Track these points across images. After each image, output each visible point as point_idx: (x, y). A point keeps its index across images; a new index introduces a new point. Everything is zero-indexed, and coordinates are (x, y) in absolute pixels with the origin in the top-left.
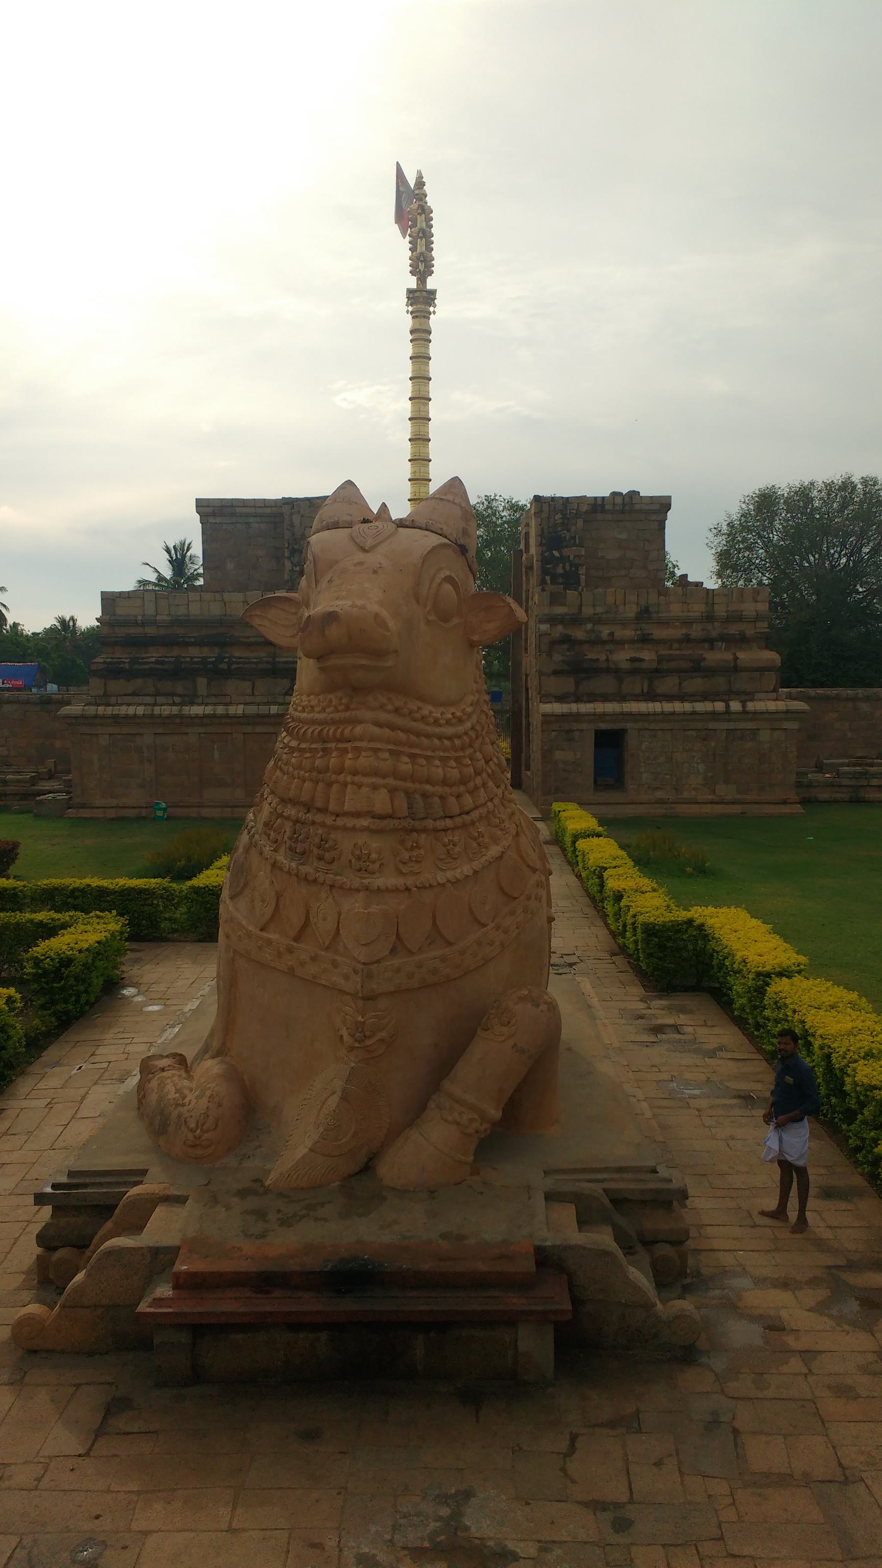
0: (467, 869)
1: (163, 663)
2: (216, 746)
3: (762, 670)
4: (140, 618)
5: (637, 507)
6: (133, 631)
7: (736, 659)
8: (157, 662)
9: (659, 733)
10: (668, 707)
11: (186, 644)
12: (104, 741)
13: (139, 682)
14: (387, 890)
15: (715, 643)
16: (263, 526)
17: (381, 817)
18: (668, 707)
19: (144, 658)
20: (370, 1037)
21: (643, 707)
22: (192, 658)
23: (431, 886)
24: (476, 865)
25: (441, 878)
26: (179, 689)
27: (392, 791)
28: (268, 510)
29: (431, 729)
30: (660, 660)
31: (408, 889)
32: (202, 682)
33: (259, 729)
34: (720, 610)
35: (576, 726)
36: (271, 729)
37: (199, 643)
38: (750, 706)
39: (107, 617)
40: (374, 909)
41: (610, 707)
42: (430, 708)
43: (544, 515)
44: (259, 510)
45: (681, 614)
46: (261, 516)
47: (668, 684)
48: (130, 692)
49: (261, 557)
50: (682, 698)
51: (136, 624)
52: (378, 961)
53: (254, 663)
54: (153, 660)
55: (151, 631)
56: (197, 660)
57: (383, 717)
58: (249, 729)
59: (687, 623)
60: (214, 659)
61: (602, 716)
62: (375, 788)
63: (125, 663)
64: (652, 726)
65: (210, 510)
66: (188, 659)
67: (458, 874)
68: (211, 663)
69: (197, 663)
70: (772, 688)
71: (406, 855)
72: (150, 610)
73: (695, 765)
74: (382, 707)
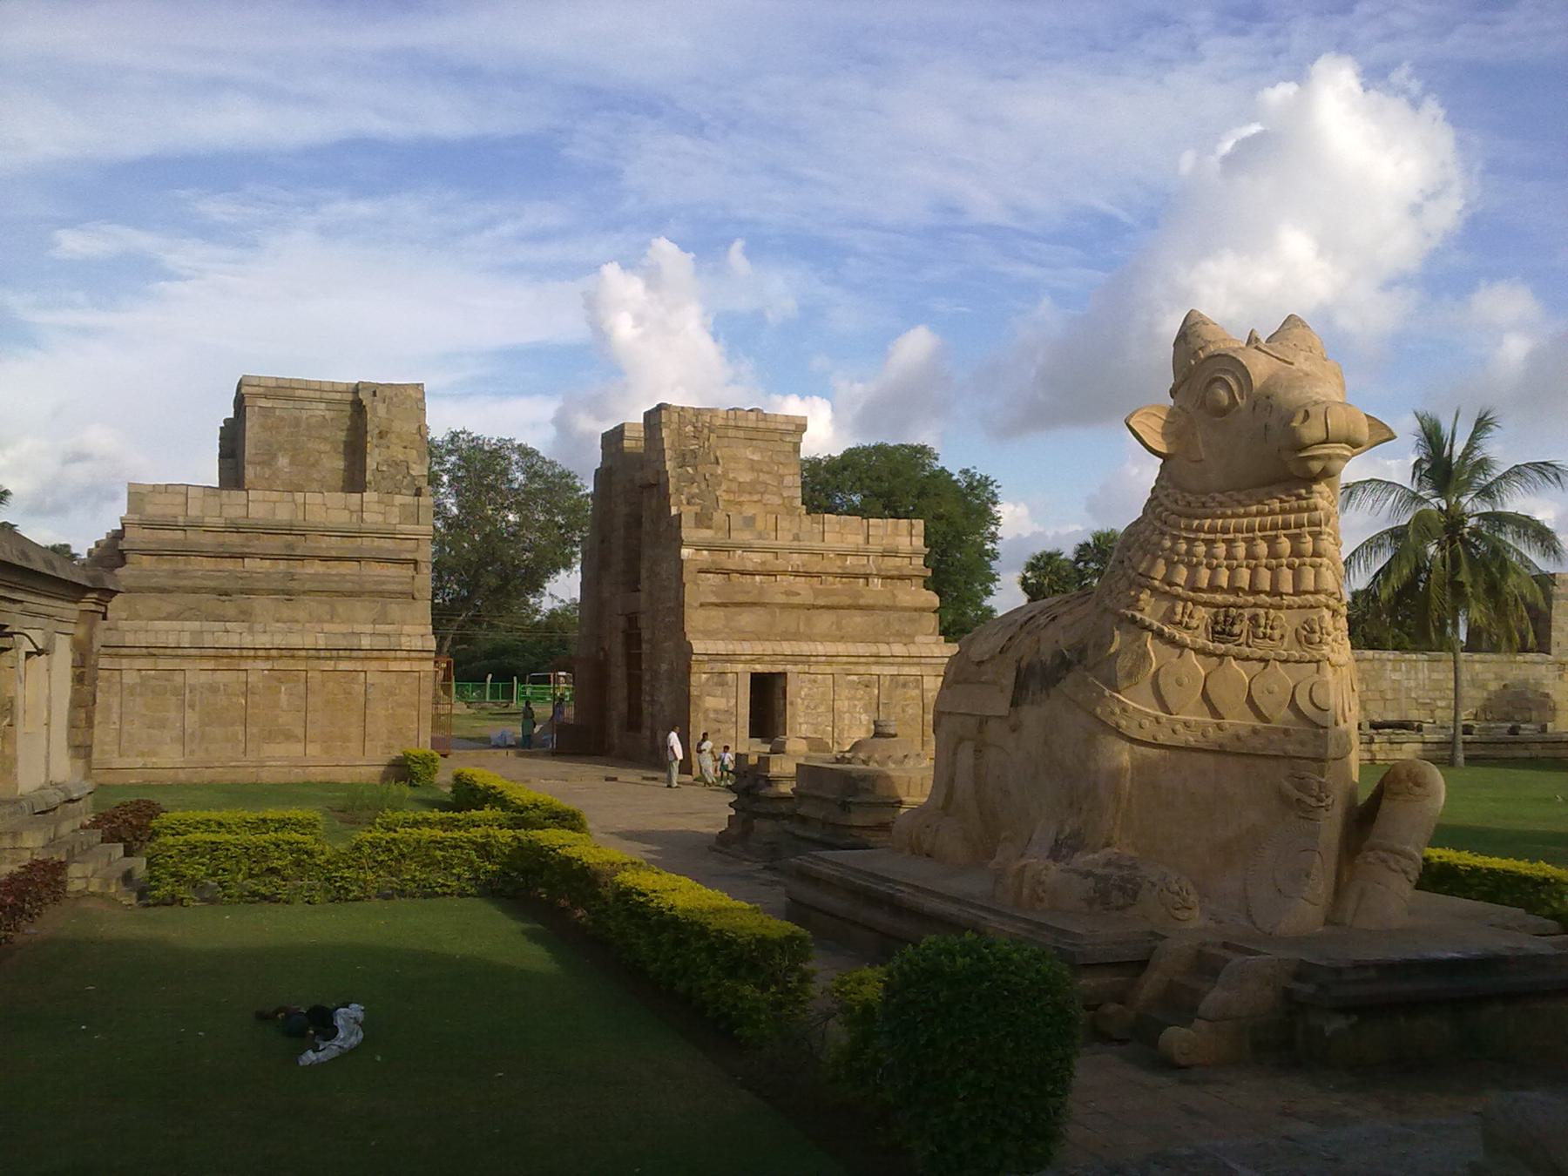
2: (283, 689)
3: (923, 610)
5: (772, 426)
7: (894, 596)
9: (819, 676)
10: (831, 648)
12: (130, 678)
15: (870, 580)
16: (329, 415)
18: (831, 648)
21: (805, 648)
28: (338, 396)
30: (816, 598)
33: (343, 665)
34: (875, 545)
35: (728, 667)
36: (358, 666)
38: (914, 650)
39: (137, 517)
41: (768, 647)
43: (674, 426)
44: (325, 395)
45: (836, 545)
46: (329, 402)
47: (824, 621)
48: (164, 615)
49: (325, 453)
50: (842, 639)
51: (174, 527)
53: (335, 581)
58: (329, 665)
59: (843, 555)
61: (758, 658)
64: (813, 669)
65: (261, 390)
70: (931, 631)
73: (858, 715)
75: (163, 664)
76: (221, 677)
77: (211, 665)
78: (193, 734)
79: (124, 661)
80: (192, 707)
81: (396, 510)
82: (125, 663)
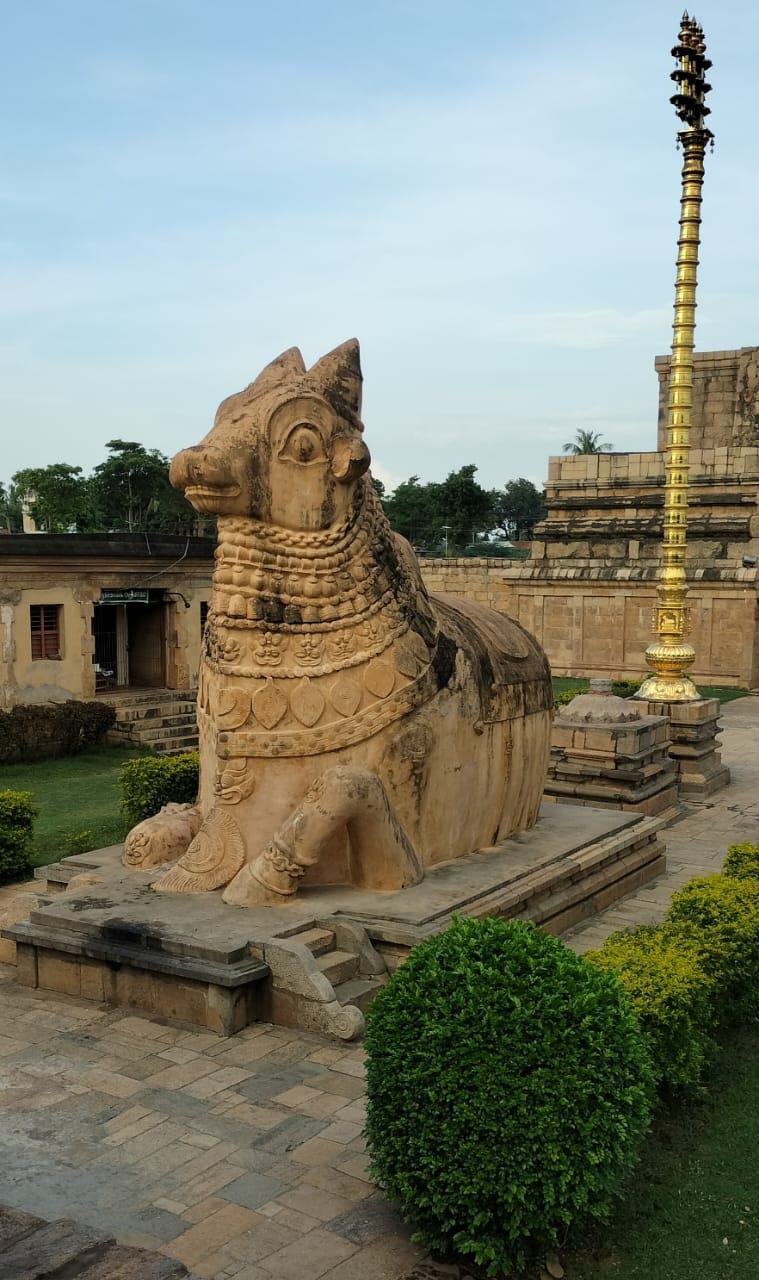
0: (326, 667)
1: (599, 526)
2: (641, 611)
4: (582, 481)
6: (575, 494)
8: (593, 525)
11: (623, 507)
12: (538, 602)
13: (576, 545)
14: (242, 676)
17: (236, 617)
19: (583, 521)
20: (225, 788)
22: (627, 521)
23: (287, 677)
24: (338, 665)
25: (297, 671)
26: (613, 553)
27: (246, 596)
29: (297, 551)
31: (263, 677)
32: (634, 545)
37: (637, 505)
39: (552, 482)
40: (231, 688)
42: (289, 532)
52: (233, 730)
54: (590, 523)
55: (591, 493)
56: (630, 522)
57: (239, 537)
60: (647, 522)
62: (231, 593)
63: (563, 526)
66: (623, 522)
67: (315, 671)
68: (644, 525)
69: (631, 526)
71: (260, 650)
72: (592, 474)
74: (237, 530)
75: (559, 592)
76: (597, 602)
77: (590, 592)
78: (578, 643)
79: (535, 589)
80: (578, 624)
81: (742, 460)
82: (535, 591)
